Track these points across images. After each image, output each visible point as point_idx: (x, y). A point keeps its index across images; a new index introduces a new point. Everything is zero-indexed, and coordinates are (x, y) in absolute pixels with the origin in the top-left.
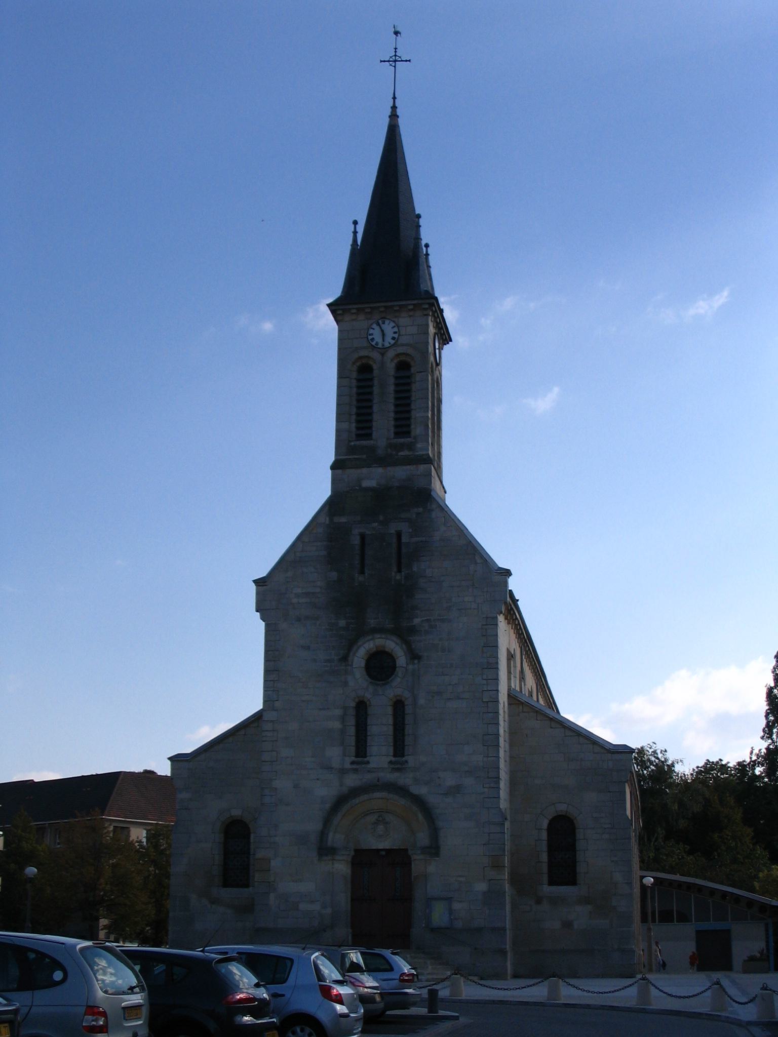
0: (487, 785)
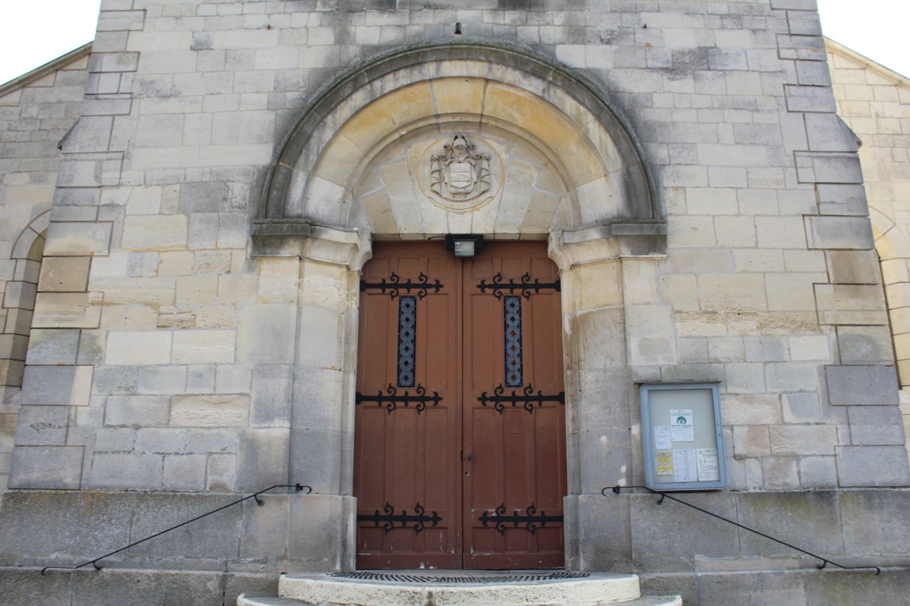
0: (792, 54)
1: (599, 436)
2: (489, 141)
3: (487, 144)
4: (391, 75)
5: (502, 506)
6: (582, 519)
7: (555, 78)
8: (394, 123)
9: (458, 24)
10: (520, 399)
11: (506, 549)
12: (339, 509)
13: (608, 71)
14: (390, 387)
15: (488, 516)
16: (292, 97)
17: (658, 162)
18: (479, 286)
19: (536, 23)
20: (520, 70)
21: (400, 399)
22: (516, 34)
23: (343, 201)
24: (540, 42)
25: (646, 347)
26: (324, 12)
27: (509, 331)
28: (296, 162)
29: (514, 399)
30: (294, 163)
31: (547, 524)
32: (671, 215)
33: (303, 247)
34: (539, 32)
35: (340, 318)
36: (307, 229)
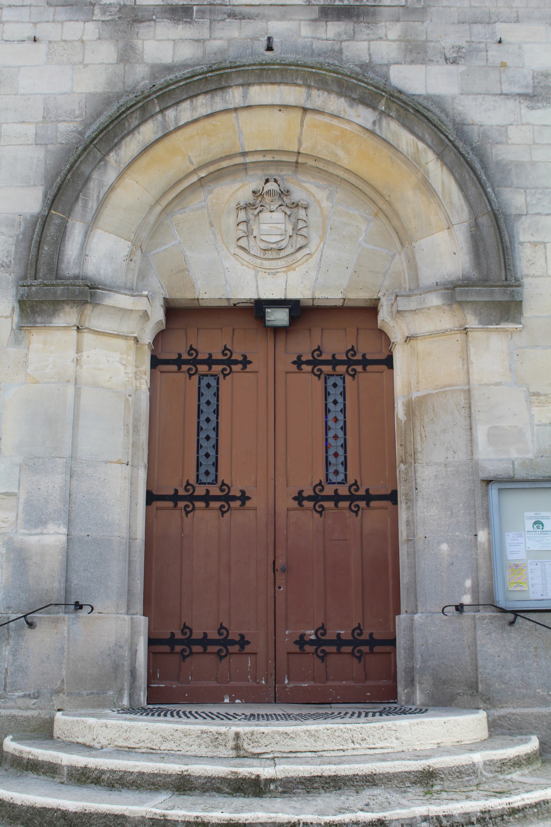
1: (439, 543)
2: (307, 185)
3: (305, 188)
4: (188, 102)
5: (323, 627)
6: (418, 643)
7: (388, 107)
8: (192, 163)
9: (269, 39)
10: (344, 498)
11: (327, 679)
12: (127, 631)
13: (453, 98)
14: (188, 484)
15: (306, 639)
16: (66, 129)
17: (513, 212)
18: (294, 363)
19: (365, 37)
20: (346, 96)
21: (200, 498)
22: (341, 51)
23: (130, 258)
24: (370, 61)
25: (496, 437)
26: (103, 21)
27: (331, 416)
28: (71, 210)
29: (337, 498)
30: (69, 212)
31: (377, 649)
32: (528, 276)
33: (81, 314)
34: (369, 49)
35: (127, 401)
36: (86, 293)
